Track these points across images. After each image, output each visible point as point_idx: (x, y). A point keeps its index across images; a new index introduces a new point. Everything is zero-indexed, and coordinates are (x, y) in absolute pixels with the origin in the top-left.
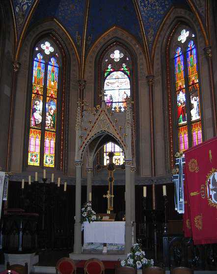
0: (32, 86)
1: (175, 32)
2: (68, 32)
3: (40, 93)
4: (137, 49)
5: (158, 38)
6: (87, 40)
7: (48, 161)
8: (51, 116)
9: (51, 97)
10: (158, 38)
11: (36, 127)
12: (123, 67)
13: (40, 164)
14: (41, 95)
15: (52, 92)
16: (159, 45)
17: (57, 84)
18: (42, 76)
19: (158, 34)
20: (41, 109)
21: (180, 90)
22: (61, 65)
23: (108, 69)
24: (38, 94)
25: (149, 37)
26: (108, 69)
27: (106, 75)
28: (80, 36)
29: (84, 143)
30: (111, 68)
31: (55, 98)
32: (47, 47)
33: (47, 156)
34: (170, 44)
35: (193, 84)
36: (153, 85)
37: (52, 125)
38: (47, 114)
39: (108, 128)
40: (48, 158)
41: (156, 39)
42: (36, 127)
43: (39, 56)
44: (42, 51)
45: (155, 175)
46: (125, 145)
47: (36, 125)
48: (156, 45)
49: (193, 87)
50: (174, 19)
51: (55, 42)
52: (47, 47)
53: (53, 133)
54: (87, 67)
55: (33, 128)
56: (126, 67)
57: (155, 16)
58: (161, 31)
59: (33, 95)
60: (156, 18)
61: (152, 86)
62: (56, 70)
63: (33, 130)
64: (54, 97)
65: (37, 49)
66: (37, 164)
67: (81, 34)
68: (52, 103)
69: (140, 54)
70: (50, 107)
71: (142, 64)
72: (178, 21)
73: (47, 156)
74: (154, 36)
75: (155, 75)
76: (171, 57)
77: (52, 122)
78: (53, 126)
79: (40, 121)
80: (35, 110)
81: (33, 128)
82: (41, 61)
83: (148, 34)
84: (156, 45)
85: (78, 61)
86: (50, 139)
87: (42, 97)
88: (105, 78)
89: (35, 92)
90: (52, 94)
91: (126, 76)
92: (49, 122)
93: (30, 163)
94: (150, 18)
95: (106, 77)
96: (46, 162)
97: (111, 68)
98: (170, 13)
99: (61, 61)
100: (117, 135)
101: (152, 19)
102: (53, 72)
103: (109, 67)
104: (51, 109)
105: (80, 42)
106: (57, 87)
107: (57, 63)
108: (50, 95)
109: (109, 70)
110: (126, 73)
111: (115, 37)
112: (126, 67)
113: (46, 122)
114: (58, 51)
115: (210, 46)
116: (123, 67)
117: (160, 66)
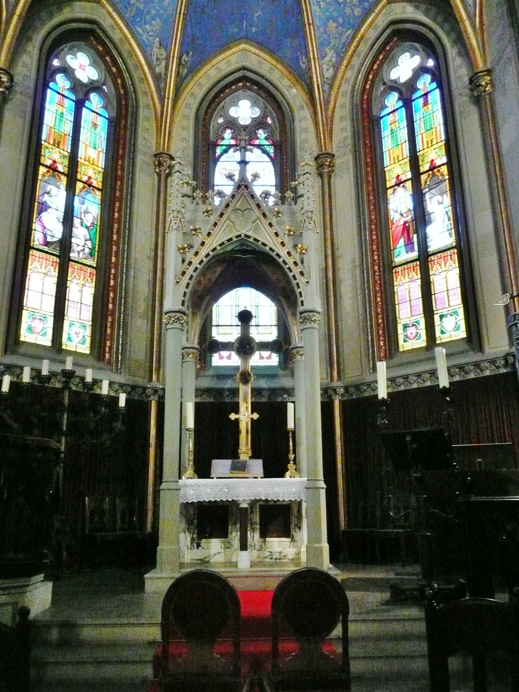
0: (39, 146)
1: (385, 58)
2: (134, 36)
3: (61, 168)
4: (295, 96)
5: (344, 72)
6: (179, 64)
7: (73, 336)
8: (87, 227)
9: (88, 184)
10: (344, 72)
11: (46, 249)
12: (257, 138)
13: (53, 341)
14: (63, 174)
15: (91, 173)
16: (347, 88)
17: (102, 156)
18: (68, 128)
19: (345, 62)
20: (62, 208)
21: (398, 185)
22: (114, 114)
23: (223, 139)
24: (55, 170)
25: (324, 66)
26: (223, 139)
27: (219, 151)
28: (163, 51)
29: (190, 263)
30: (232, 138)
31: (98, 189)
32: (81, 66)
33: (71, 325)
34: (372, 86)
35: (433, 168)
36: (333, 174)
37: (87, 251)
38: (77, 222)
39: (257, 229)
40: (75, 329)
41: (340, 76)
42: (46, 249)
43: (60, 78)
44: (67, 71)
45: (339, 378)
46: (302, 273)
47: (47, 243)
48: (339, 88)
49: (434, 174)
50: (388, 27)
51: (102, 56)
52: (81, 66)
53: (89, 270)
54: (178, 118)
55: (37, 250)
56: (266, 139)
57: (341, 20)
58: (352, 56)
59: (42, 170)
60: (342, 25)
61: (330, 177)
62: (103, 124)
63: (37, 254)
64: (95, 184)
65: (56, 63)
66: (47, 341)
67: (164, 44)
68: (89, 197)
69: (302, 108)
70: (84, 207)
71: (306, 130)
72: (395, 33)
73: (71, 325)
74: (337, 67)
75: (334, 152)
76: (375, 113)
77: (89, 243)
78: (91, 255)
79: (58, 235)
80: (44, 207)
81: (37, 250)
82: (66, 93)
83: (323, 58)
84: (339, 88)
85: (155, 110)
86: (82, 282)
87: (64, 179)
88: (217, 160)
89: (49, 162)
90: (90, 178)
91: (266, 158)
92: (82, 242)
93: (25, 336)
94: (331, 21)
95: (220, 156)
96: (70, 339)
97: (232, 138)
98: (378, 15)
99: (115, 104)
100: (279, 246)
101: (335, 25)
102: (95, 125)
103: (228, 134)
104: (86, 212)
105: (163, 63)
106: (102, 163)
107: (105, 107)
108: (85, 179)
109: (226, 142)
110: (264, 152)
111: (244, 68)
112: (266, 139)
113: (73, 240)
114: (109, 81)
115: (489, 66)
116: (257, 138)
117: (349, 133)
